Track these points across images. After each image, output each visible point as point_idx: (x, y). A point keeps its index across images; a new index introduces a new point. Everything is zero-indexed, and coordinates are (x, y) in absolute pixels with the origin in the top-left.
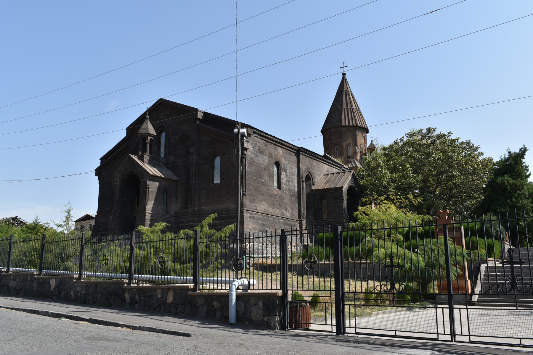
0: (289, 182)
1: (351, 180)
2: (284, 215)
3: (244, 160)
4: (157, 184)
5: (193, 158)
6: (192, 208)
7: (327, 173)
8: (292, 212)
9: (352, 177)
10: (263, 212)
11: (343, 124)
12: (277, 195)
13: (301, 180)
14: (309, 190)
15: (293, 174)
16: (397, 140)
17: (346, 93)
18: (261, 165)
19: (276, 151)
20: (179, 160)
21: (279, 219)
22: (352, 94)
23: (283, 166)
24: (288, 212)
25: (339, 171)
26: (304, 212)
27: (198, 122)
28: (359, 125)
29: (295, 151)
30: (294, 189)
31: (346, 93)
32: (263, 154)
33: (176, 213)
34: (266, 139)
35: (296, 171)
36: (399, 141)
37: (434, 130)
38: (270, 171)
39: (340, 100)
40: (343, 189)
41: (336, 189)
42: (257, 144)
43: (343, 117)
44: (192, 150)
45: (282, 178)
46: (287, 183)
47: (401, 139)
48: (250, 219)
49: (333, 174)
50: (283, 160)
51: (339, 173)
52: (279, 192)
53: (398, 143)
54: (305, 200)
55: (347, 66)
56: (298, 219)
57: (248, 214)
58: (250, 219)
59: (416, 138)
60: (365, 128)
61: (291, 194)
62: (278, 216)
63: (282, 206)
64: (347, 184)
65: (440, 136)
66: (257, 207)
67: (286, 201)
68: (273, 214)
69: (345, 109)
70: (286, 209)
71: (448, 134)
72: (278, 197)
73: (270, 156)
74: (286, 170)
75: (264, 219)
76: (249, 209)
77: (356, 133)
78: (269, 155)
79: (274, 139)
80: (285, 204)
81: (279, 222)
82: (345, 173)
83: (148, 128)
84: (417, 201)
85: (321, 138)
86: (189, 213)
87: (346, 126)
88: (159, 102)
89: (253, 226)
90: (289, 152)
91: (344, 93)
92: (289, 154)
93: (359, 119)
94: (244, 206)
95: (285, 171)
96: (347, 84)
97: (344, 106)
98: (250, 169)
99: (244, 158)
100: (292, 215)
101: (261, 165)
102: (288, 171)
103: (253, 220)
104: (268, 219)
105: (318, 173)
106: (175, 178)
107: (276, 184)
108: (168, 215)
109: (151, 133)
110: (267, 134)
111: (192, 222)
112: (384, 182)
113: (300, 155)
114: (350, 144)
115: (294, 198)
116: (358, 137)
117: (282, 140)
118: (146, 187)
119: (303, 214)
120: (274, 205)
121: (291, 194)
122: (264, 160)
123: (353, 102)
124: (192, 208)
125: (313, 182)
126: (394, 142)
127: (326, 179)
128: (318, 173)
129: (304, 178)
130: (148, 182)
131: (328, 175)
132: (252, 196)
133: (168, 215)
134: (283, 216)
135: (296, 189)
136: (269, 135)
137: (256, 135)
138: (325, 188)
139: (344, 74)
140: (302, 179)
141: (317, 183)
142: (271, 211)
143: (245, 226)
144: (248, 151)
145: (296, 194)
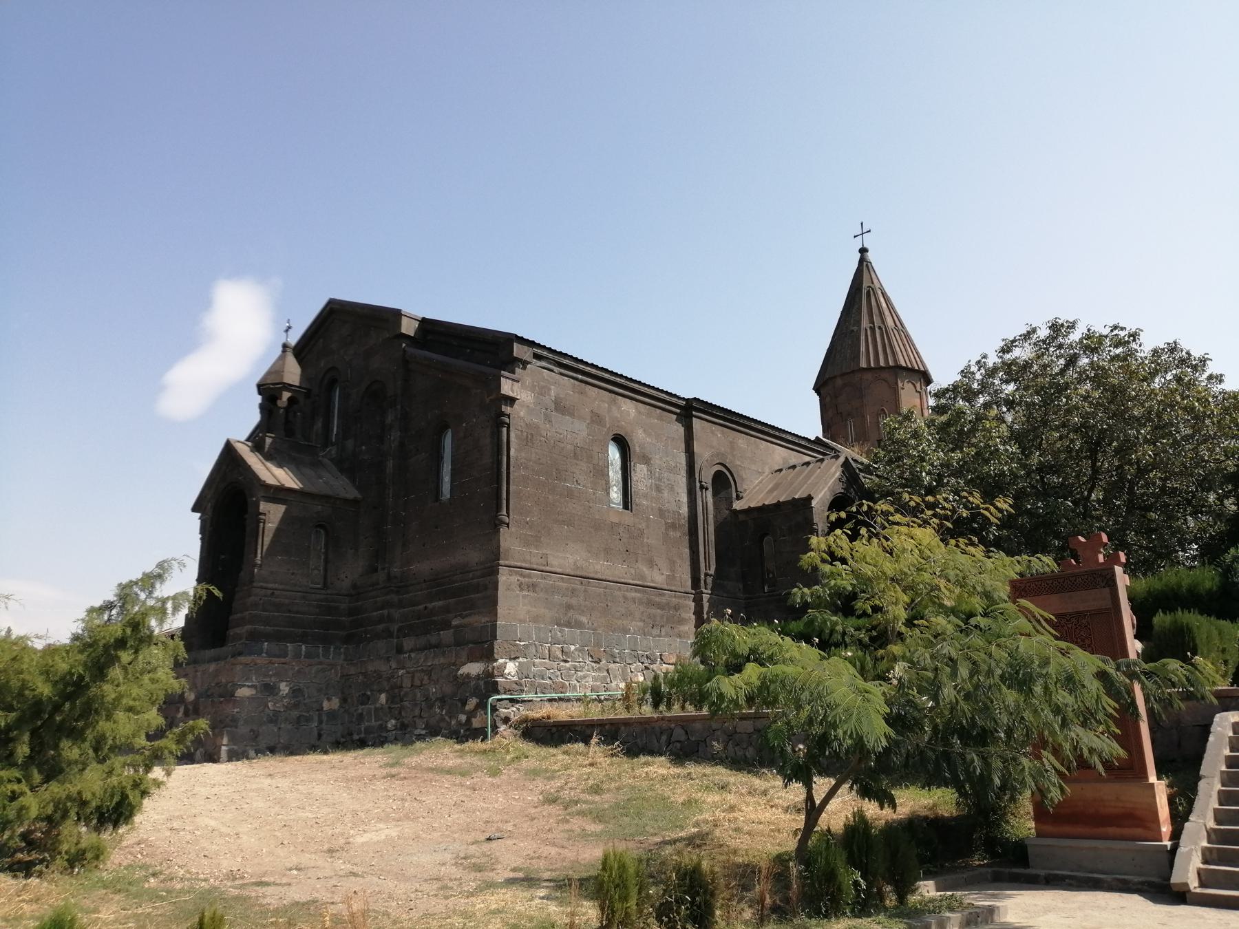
0: (658, 489)
1: (840, 480)
2: (643, 577)
3: (505, 430)
4: (282, 508)
5: (392, 438)
6: (386, 571)
7: (777, 468)
8: (673, 570)
9: (843, 472)
10: (568, 571)
11: (863, 364)
12: (619, 524)
13: (698, 485)
14: (727, 512)
15: (671, 470)
16: (969, 366)
17: (868, 293)
18: (562, 445)
19: (614, 408)
20: (364, 448)
21: (627, 590)
22: (884, 294)
23: (637, 449)
24: (656, 570)
25: (807, 459)
26: (709, 567)
27: (404, 345)
28: (904, 365)
29: (678, 411)
30: (676, 509)
31: (868, 293)
32: (572, 415)
33: (354, 586)
34: (580, 377)
35: (684, 462)
36: (974, 369)
37: (1072, 326)
38: (595, 462)
39: (854, 311)
40: (814, 503)
41: (794, 503)
42: (550, 389)
43: (863, 348)
44: (389, 418)
45: (634, 478)
46: (654, 494)
47: (978, 362)
48: (522, 590)
49: (794, 467)
50: (640, 431)
51: (808, 464)
52: (628, 518)
53: (973, 373)
54: (712, 537)
55: (869, 231)
56: (690, 590)
57: (514, 578)
58: (522, 590)
59: (1017, 353)
60: (919, 371)
61: (666, 523)
62: (623, 580)
63: (636, 554)
64: (826, 489)
65: (1092, 343)
66: (550, 559)
67: (653, 539)
68: (604, 578)
69: (866, 330)
70: (651, 563)
71: (1112, 331)
72: (621, 530)
73: (592, 421)
74: (650, 459)
75: (573, 591)
76: (519, 564)
77: (897, 384)
78: (591, 417)
79: (607, 376)
80: (646, 549)
81: (625, 598)
82: (822, 460)
83: (283, 372)
84: (996, 508)
85: (813, 402)
86: (378, 584)
87: (869, 369)
88: (328, 308)
89: (529, 612)
90: (658, 411)
91: (864, 292)
92: (660, 418)
93: (903, 350)
94: (502, 555)
95: (646, 460)
96: (872, 273)
97: (865, 323)
98: (523, 454)
99: (506, 424)
100: (671, 578)
101: (562, 445)
102: (657, 460)
103: (531, 594)
104: (585, 591)
105: (753, 467)
106: (352, 493)
107: (616, 495)
108: (329, 592)
109: (291, 382)
110: (582, 362)
111: (382, 608)
112: (924, 474)
113: (694, 419)
114: (883, 410)
115: (679, 534)
116: (902, 393)
117: (630, 379)
118: (258, 518)
119: (706, 575)
120: (607, 552)
121: (666, 523)
122: (575, 430)
123: (887, 313)
124: (386, 571)
125: (737, 491)
126: (962, 371)
127: (774, 482)
128: (753, 467)
129: (707, 479)
130: (263, 506)
131: (780, 470)
132: (531, 528)
133: (329, 592)
134: (638, 582)
135: (684, 510)
136: (586, 364)
137: (543, 364)
138: (766, 503)
139: (863, 251)
140: (700, 482)
141: (749, 494)
142: (598, 567)
143: (499, 611)
144: (515, 406)
145: (684, 522)
